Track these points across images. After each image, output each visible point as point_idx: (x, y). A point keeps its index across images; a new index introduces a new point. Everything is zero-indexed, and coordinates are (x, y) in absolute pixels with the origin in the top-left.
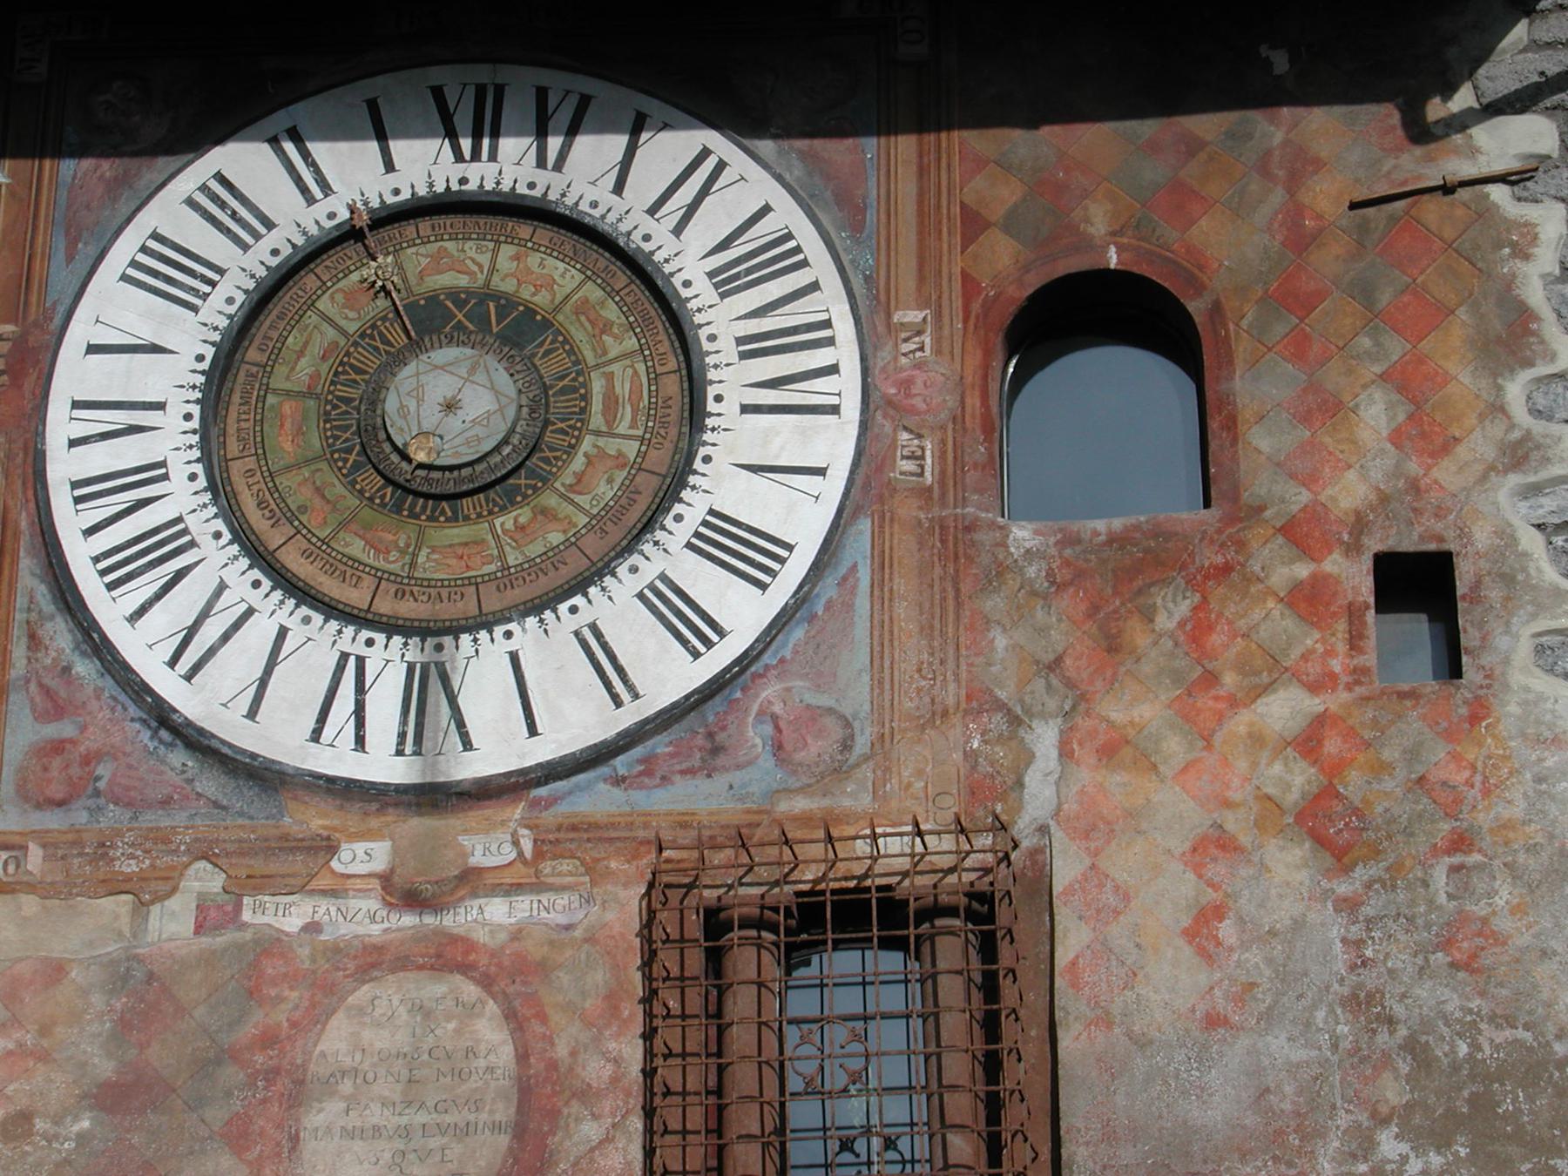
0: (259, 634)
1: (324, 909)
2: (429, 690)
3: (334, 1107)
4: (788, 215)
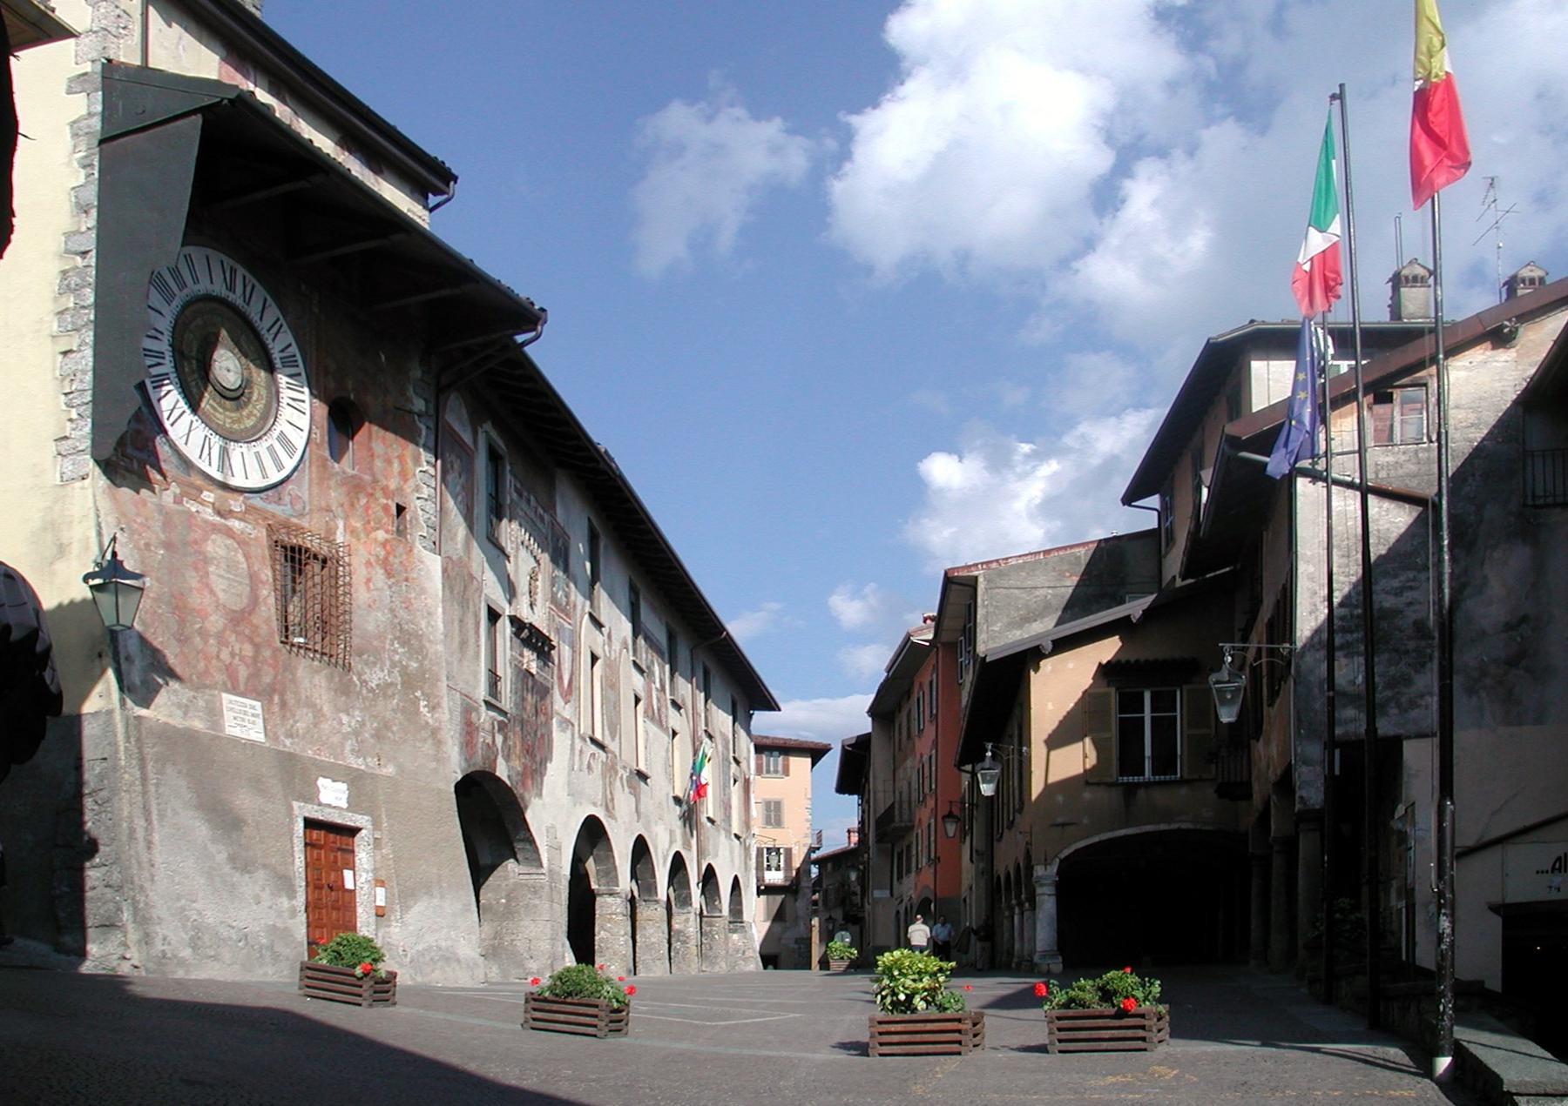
1: (201, 508)
2: (224, 452)
4: (294, 349)
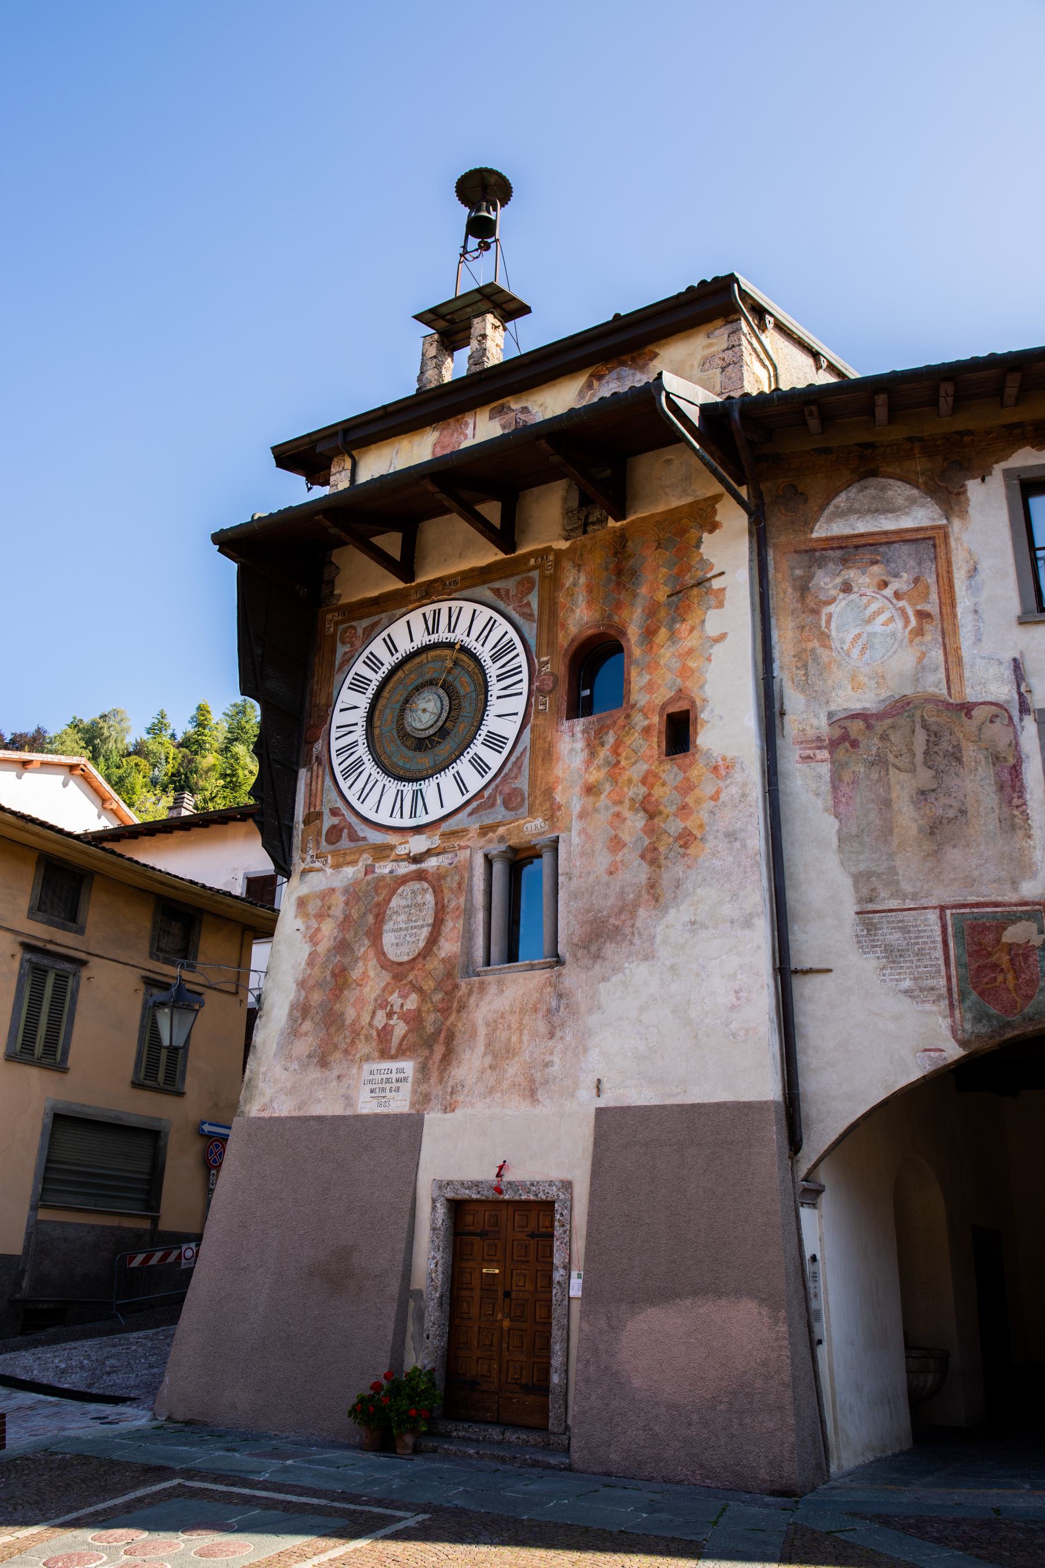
0: (378, 787)
3: (392, 923)
4: (513, 634)
